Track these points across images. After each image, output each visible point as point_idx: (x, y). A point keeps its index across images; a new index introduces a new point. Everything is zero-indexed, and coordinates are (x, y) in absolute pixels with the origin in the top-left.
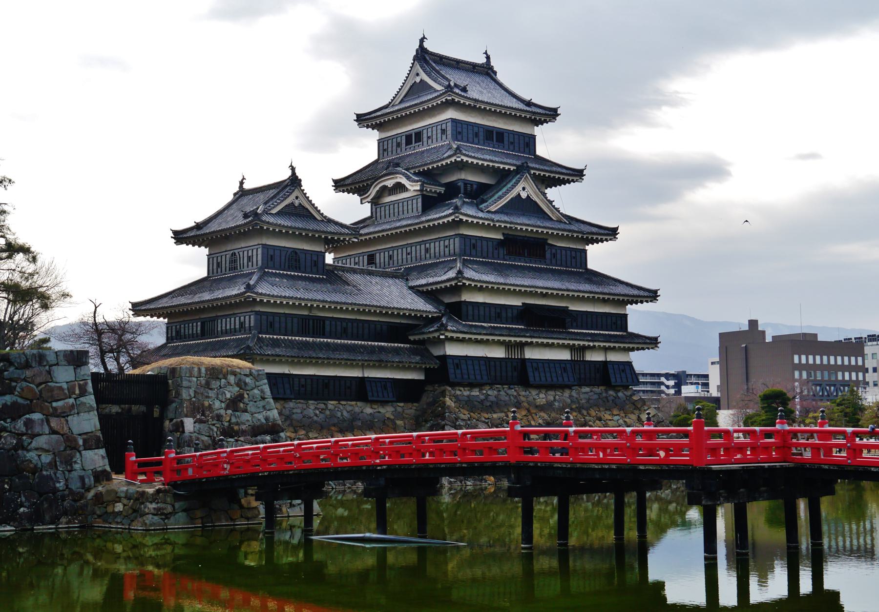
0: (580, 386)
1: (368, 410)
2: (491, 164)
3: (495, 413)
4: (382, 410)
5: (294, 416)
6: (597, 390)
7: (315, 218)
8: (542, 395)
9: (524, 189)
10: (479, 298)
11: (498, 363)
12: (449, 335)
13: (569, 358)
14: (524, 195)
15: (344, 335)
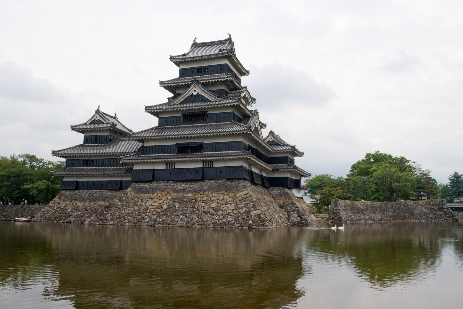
0: (209, 180)
1: (109, 193)
2: (178, 84)
3: (148, 193)
4: (115, 193)
5: (75, 196)
6: (220, 181)
7: (104, 123)
8: (183, 185)
9: (195, 91)
10: (153, 144)
11: (162, 172)
12: (124, 161)
13: (202, 166)
14: (195, 94)
15: (102, 164)
